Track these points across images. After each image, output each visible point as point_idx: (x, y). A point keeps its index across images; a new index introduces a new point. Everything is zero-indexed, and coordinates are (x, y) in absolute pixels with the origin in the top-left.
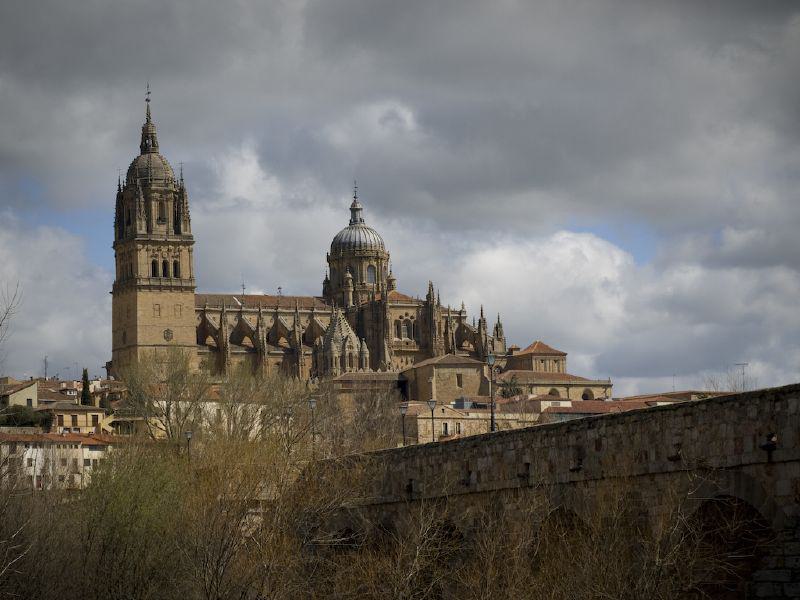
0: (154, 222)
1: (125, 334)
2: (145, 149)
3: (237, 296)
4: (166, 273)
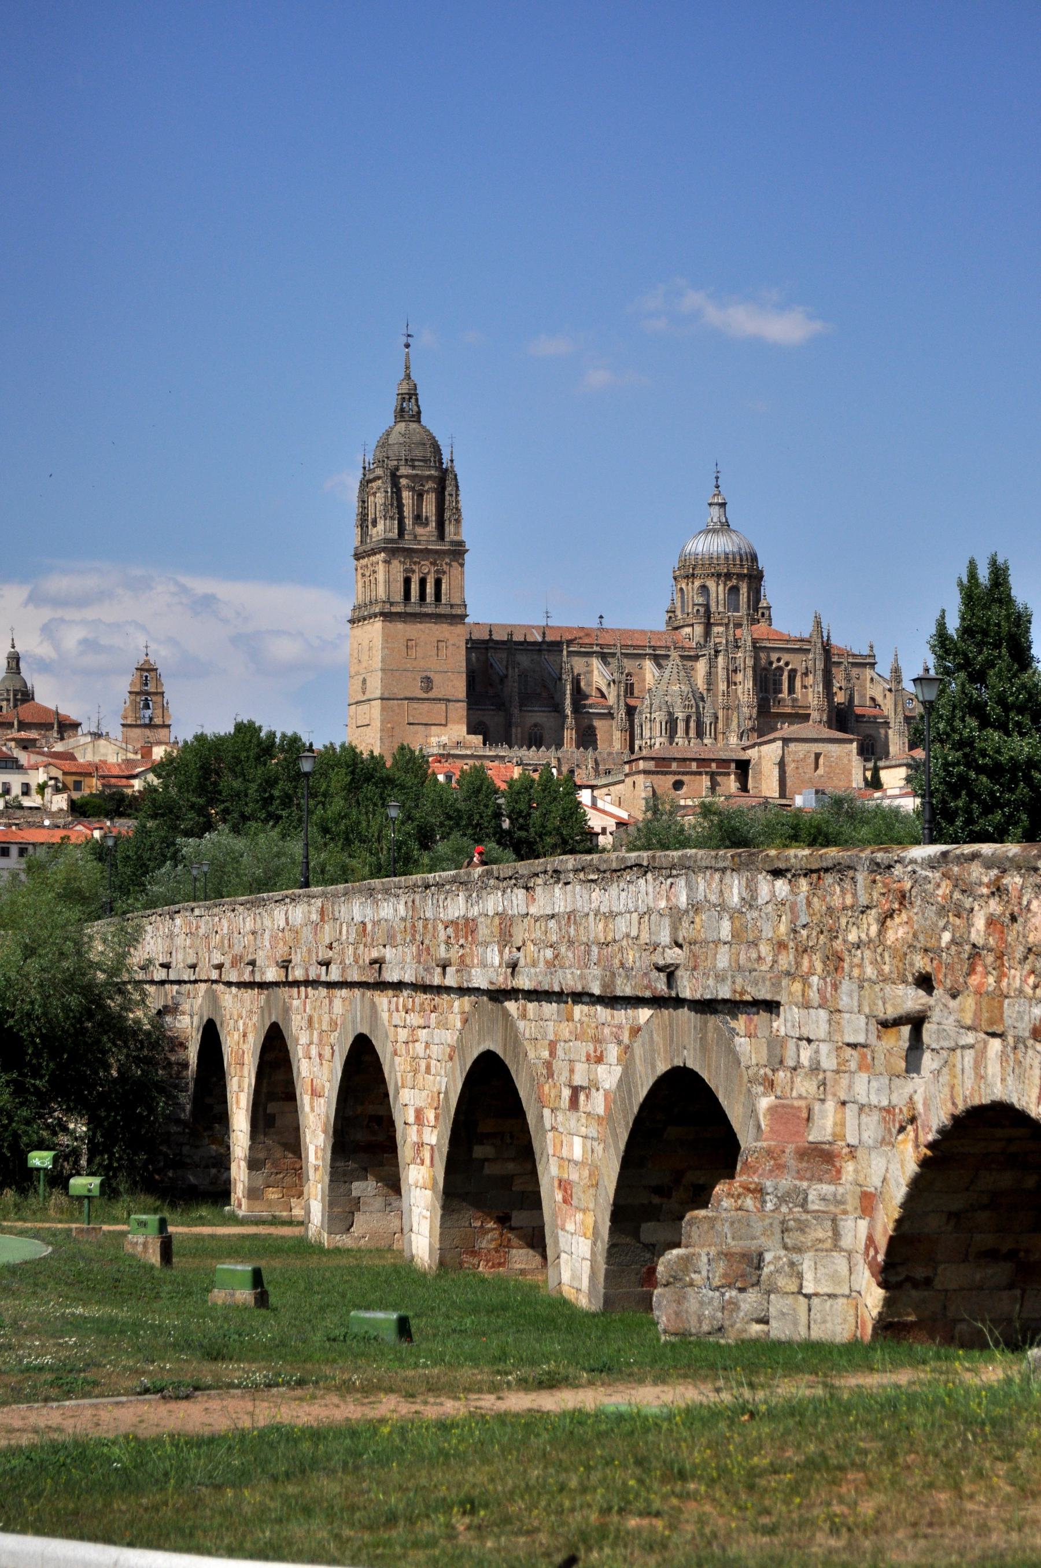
0: (408, 522)
1: (364, 681)
2: (401, 414)
3: (537, 628)
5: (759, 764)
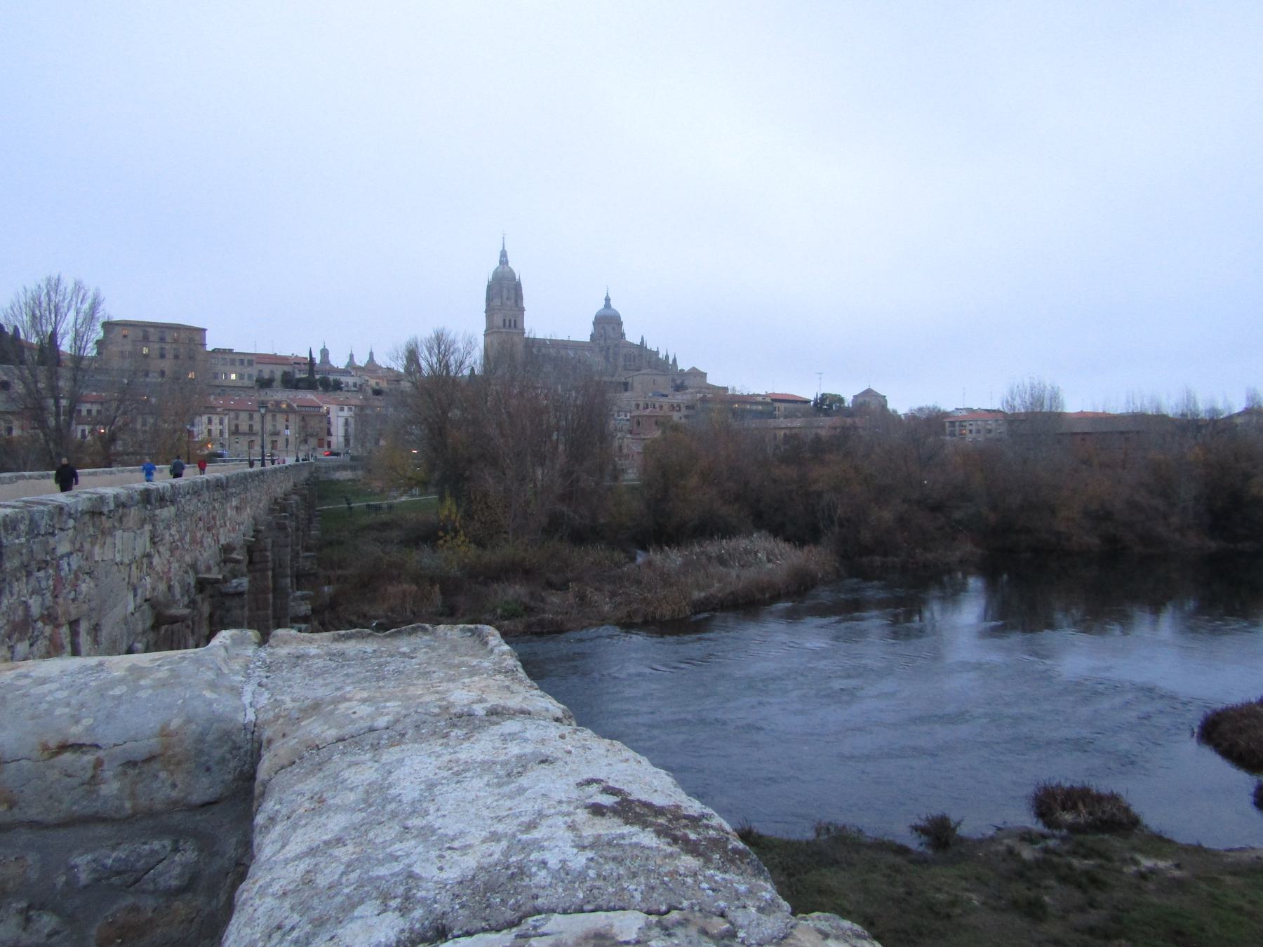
2: (501, 262)
4: (510, 326)
5: (632, 384)
